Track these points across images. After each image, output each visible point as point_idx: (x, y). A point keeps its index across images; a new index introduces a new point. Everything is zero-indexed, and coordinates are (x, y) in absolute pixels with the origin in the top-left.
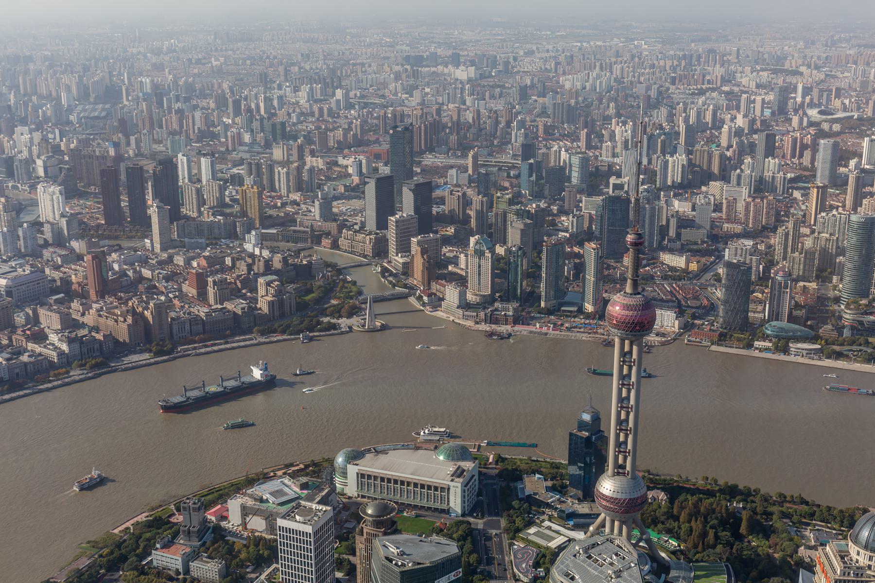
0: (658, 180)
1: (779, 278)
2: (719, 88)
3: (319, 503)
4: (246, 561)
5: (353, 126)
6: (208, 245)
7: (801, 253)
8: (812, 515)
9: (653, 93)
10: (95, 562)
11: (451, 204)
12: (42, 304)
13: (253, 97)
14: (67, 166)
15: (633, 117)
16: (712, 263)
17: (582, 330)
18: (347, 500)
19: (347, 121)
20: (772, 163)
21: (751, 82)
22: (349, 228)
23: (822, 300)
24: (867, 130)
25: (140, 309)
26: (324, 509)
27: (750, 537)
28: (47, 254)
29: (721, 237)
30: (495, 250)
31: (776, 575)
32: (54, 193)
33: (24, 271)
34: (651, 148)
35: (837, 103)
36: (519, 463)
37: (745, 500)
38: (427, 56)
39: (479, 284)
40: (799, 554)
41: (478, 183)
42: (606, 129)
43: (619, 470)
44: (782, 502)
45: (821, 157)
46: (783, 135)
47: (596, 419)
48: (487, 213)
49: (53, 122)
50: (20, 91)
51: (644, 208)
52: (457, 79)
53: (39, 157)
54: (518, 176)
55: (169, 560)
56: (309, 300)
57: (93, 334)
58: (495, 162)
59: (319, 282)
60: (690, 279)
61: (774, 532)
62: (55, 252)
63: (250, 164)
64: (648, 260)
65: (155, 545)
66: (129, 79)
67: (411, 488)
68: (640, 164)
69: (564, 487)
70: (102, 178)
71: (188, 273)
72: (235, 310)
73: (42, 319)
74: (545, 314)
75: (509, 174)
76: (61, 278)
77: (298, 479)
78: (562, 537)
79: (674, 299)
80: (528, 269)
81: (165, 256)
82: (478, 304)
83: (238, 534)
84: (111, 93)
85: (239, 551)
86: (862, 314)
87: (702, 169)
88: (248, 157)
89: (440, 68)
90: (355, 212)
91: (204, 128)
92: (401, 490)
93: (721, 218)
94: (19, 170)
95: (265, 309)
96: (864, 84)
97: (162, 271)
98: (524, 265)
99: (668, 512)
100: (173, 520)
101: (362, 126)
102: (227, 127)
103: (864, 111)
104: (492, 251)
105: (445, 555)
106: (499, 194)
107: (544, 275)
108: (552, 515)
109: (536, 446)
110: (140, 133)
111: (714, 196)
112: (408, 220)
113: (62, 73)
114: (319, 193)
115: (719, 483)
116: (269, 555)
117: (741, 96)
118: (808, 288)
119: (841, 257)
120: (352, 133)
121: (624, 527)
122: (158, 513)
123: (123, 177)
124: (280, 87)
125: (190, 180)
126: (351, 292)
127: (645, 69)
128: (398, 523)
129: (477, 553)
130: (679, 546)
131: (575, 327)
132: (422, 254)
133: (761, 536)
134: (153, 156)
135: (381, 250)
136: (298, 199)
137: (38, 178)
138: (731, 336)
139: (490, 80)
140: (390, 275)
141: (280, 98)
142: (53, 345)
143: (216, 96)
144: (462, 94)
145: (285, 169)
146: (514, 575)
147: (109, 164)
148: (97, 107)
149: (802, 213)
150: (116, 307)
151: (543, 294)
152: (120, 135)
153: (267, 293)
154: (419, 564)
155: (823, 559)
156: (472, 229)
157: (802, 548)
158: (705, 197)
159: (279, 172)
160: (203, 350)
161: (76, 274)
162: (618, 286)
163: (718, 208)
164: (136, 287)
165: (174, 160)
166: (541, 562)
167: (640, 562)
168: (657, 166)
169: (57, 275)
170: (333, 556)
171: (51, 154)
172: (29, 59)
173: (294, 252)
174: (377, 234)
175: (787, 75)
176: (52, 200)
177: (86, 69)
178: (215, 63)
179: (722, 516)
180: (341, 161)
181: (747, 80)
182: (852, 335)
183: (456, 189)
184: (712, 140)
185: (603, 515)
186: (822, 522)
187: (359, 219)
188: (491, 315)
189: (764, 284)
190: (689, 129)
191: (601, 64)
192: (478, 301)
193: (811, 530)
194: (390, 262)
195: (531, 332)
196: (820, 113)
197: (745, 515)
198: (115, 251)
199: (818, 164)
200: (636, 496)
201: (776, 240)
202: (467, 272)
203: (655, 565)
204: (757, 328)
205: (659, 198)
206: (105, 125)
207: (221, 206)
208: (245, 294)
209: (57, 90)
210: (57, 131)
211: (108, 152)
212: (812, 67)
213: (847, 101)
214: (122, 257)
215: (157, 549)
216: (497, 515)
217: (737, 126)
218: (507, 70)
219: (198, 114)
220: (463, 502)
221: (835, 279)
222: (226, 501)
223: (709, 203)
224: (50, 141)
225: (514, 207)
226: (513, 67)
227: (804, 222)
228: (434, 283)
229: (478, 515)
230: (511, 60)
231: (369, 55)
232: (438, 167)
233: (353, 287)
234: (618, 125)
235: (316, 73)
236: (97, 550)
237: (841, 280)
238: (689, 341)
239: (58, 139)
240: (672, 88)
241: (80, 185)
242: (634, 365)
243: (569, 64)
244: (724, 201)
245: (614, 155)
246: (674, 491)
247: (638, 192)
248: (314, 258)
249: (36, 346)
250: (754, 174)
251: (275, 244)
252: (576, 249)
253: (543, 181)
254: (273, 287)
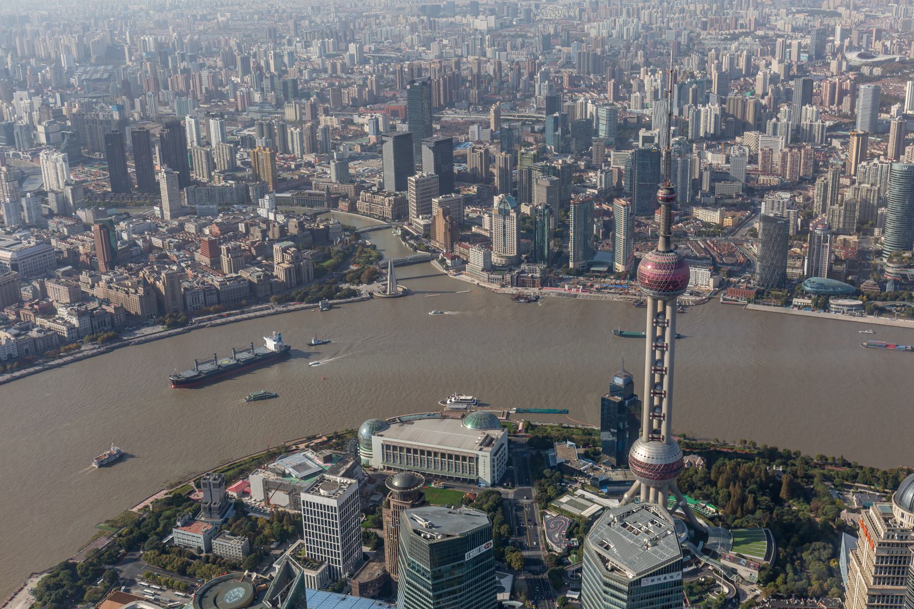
0: (690, 132)
1: (818, 232)
2: (753, 32)
3: (343, 476)
4: (270, 537)
5: (369, 82)
6: (220, 212)
7: (841, 205)
8: (854, 477)
9: (683, 40)
10: (114, 542)
11: (473, 162)
12: (50, 277)
13: (262, 54)
14: (70, 132)
15: (663, 65)
16: (747, 218)
17: (613, 291)
18: (373, 472)
19: (361, 77)
20: (809, 111)
21: (786, 25)
22: (367, 190)
23: (863, 254)
24: (909, 73)
25: (152, 280)
26: (349, 482)
27: (791, 501)
28: (52, 224)
29: (757, 190)
30: (520, 208)
31: (817, 540)
32: (57, 159)
33: (29, 243)
34: (682, 98)
35: (878, 45)
36: (549, 430)
37: (785, 464)
38: (444, 5)
39: (505, 245)
40: (842, 518)
41: (501, 139)
42: (634, 78)
43: (654, 435)
44: (824, 465)
45: (861, 103)
46: (821, 80)
47: (629, 383)
48: (511, 170)
49: (54, 85)
50: (17, 54)
51: (676, 162)
52: (476, 30)
53: (40, 123)
54: (543, 131)
55: (190, 538)
56: (328, 267)
57: (104, 307)
58: (518, 116)
59: (337, 247)
60: (725, 235)
61: (815, 495)
62: (61, 223)
63: (262, 124)
64: (681, 216)
65: (175, 523)
66: (131, 38)
67: (439, 458)
68: (670, 115)
69: (597, 453)
70: (106, 143)
71: (200, 241)
72: (250, 278)
73: (50, 293)
74: (574, 275)
75: (533, 129)
76: (68, 250)
77: (321, 451)
78: (596, 505)
79: (709, 256)
80: (555, 229)
81: (175, 223)
82: (503, 266)
83: (260, 509)
84: (113, 53)
85: (263, 528)
86: (905, 267)
87: (735, 118)
88: (259, 118)
89: (458, 18)
90: (373, 173)
91: (212, 88)
92: (428, 461)
93: (756, 170)
94: (20, 138)
95: (282, 277)
96: (907, 24)
97: (173, 240)
98: (551, 224)
99: (705, 477)
100: (192, 496)
101: (377, 81)
102: (236, 86)
103: (906, 53)
104: (517, 210)
105: (475, 527)
106: (523, 151)
107: (572, 234)
108: (585, 483)
109: (567, 412)
110: (145, 95)
111: (749, 147)
112: (428, 180)
113: (62, 33)
114: (335, 154)
115: (758, 446)
116: (293, 531)
117: (776, 40)
118: (848, 242)
119: (883, 209)
120: (367, 89)
121: (660, 494)
122: (177, 490)
123: (129, 142)
124: (290, 43)
125: (199, 143)
126: (370, 256)
127: (674, 14)
128: (426, 495)
129: (508, 523)
130: (717, 512)
131: (606, 288)
132: (444, 215)
133: (801, 500)
134: (159, 118)
135: (400, 212)
136: (313, 160)
137: (40, 145)
138: (769, 293)
139: (511, 29)
140: (411, 238)
141: (291, 54)
142: (63, 319)
143: (223, 54)
144: (481, 45)
145: (298, 130)
146: (547, 545)
147: (114, 129)
148: (99, 68)
149: (842, 163)
150: (127, 278)
151: (572, 254)
152: (124, 98)
153: (283, 260)
154: (448, 536)
155: (867, 522)
156: (495, 188)
157: (845, 511)
158: (740, 148)
159: (292, 132)
160: (219, 321)
161: (83, 245)
162: (650, 244)
163: (753, 159)
164: (147, 257)
165: (182, 122)
166: (574, 531)
167: (678, 528)
168: (688, 116)
169: (63, 246)
170: (359, 530)
171: (52, 120)
172: (25, 19)
173: (310, 216)
174: (396, 195)
175: (824, 17)
176: (56, 168)
177: (86, 28)
178: (220, 19)
179: (761, 480)
180: (357, 119)
181: (782, 23)
182: (895, 289)
183: (478, 146)
184: (746, 88)
185: (637, 482)
186: (866, 483)
187: (377, 180)
188: (517, 277)
189: (802, 239)
190: (721, 76)
191: (628, 10)
192: (504, 263)
193: (853, 492)
194: (410, 225)
195: (559, 294)
196: (860, 56)
197: (785, 479)
198: (123, 220)
199: (859, 111)
200: (672, 462)
201: (814, 192)
202: (491, 233)
203: (692, 532)
204: (795, 285)
205: (691, 151)
206: (108, 87)
207: (232, 170)
208: (260, 262)
209: (56, 52)
210: (58, 95)
211: (112, 116)
212: (851, 8)
213: (888, 43)
214: (131, 226)
215: (177, 527)
216: (528, 484)
217: (772, 72)
218: (529, 19)
219: (205, 73)
220: (493, 472)
221: (877, 231)
222: (247, 477)
223: (743, 155)
224: (51, 105)
225: (539, 164)
226: (535, 15)
227: (843, 172)
228: (457, 245)
229: (508, 485)
230: (533, 8)
231: (383, 6)
232: (458, 123)
233: (373, 251)
234: (647, 74)
235: (329, 27)
236: (116, 530)
237: (883, 232)
238: (724, 299)
239: (59, 104)
240: (704, 34)
241: (84, 151)
242: (668, 326)
243: (594, 10)
244: (760, 152)
245: (643, 106)
246: (711, 455)
247: (669, 145)
248: (331, 222)
249: (45, 321)
250: (790, 123)
251: (291, 208)
252: (605, 207)
253: (569, 136)
254: (289, 254)
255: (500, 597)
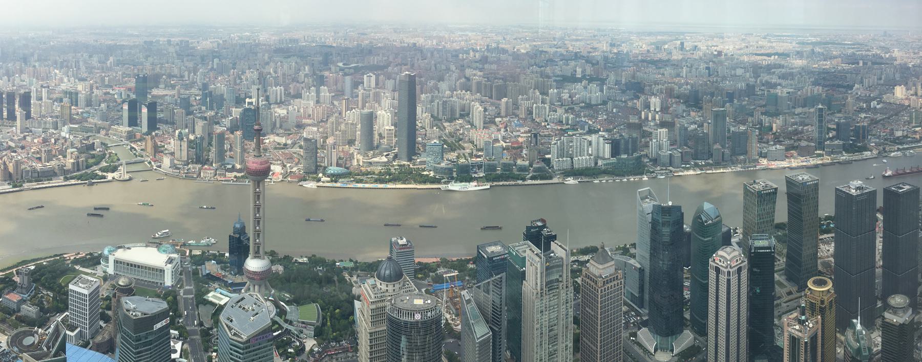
75: (196, 99)
101: (122, 75)
105: (160, 309)
154: (145, 314)
203: (278, 310)
255: (173, 356)
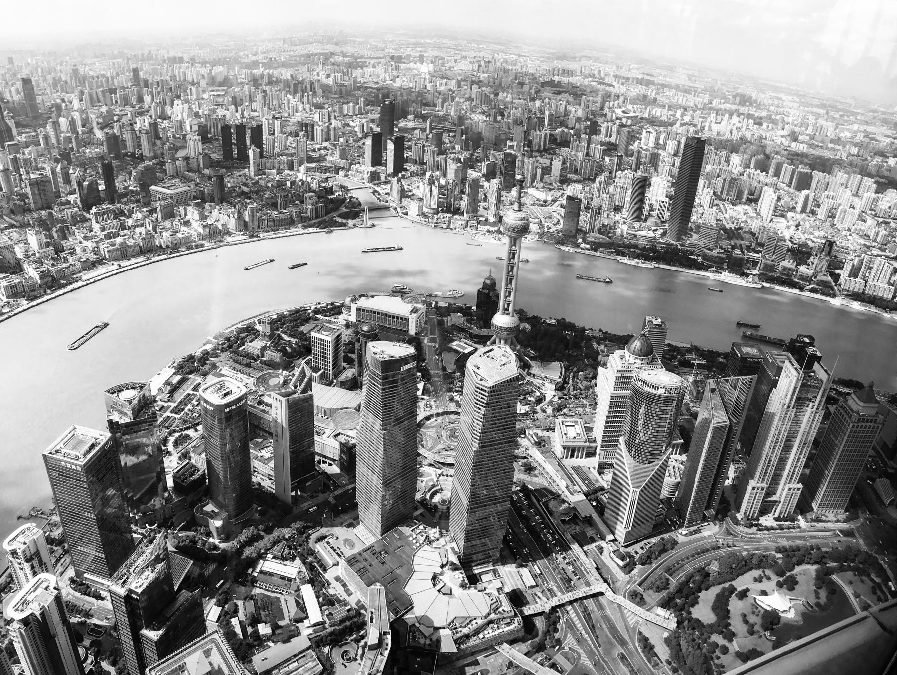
180: (351, 123)
